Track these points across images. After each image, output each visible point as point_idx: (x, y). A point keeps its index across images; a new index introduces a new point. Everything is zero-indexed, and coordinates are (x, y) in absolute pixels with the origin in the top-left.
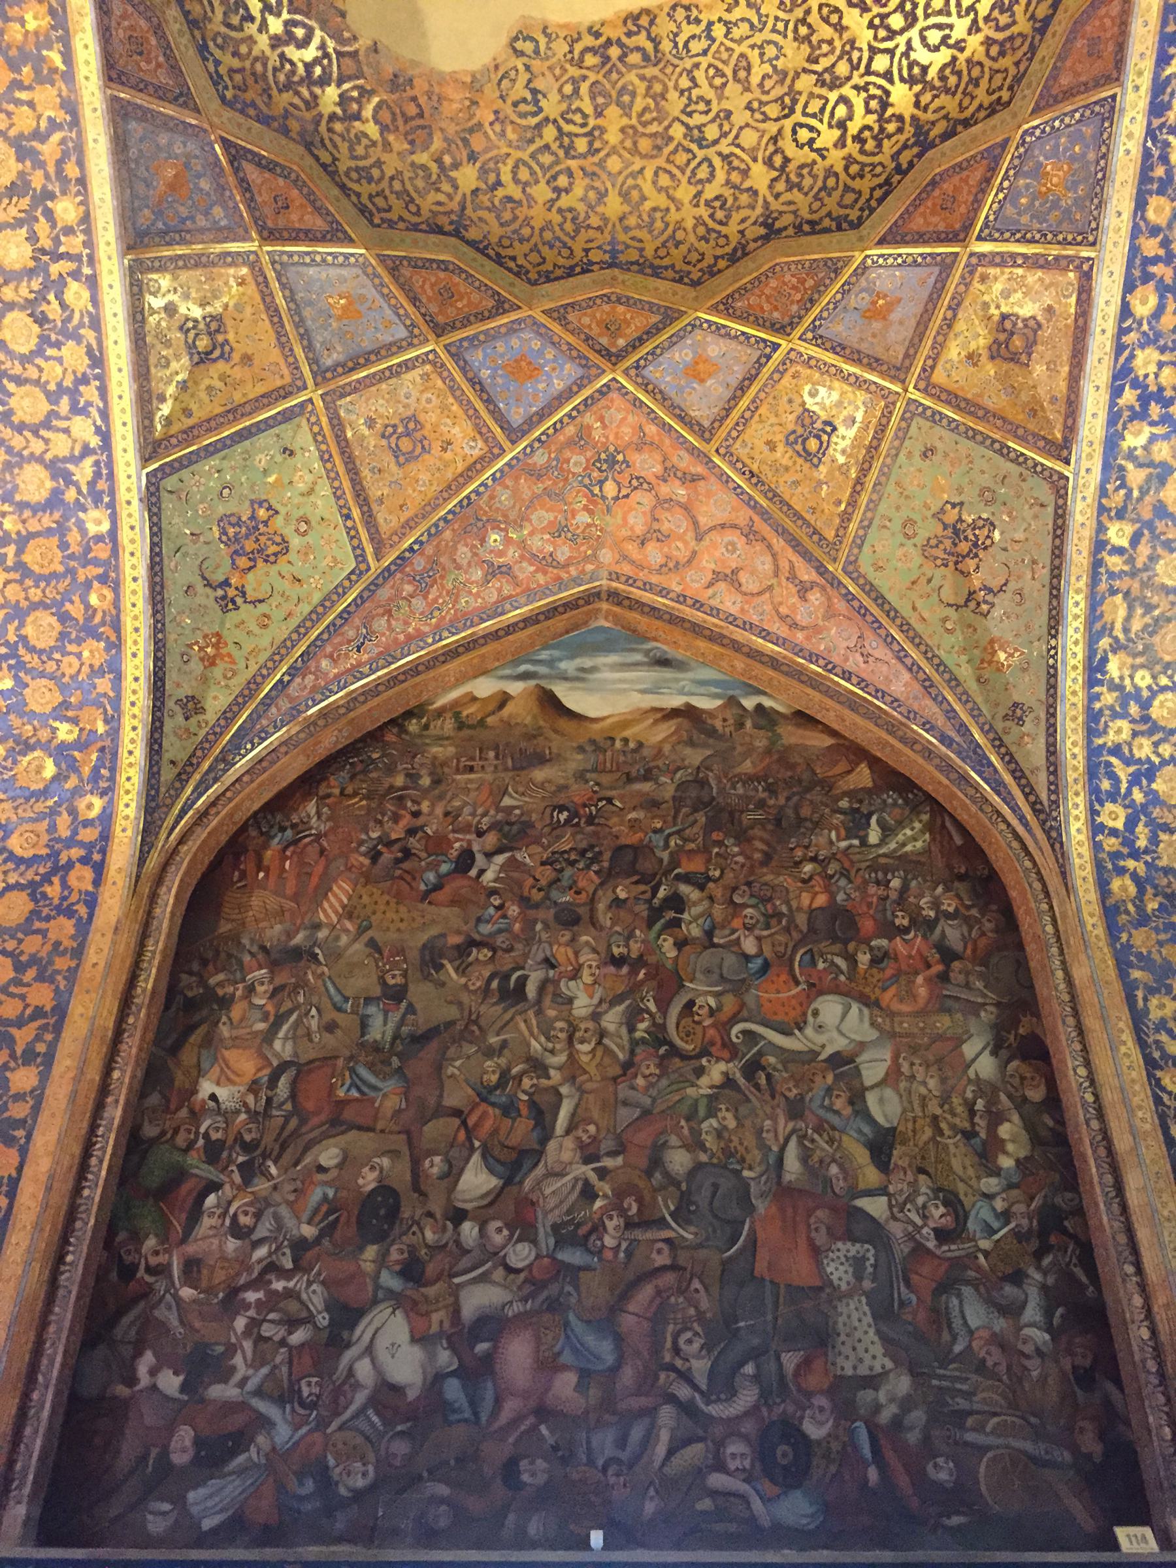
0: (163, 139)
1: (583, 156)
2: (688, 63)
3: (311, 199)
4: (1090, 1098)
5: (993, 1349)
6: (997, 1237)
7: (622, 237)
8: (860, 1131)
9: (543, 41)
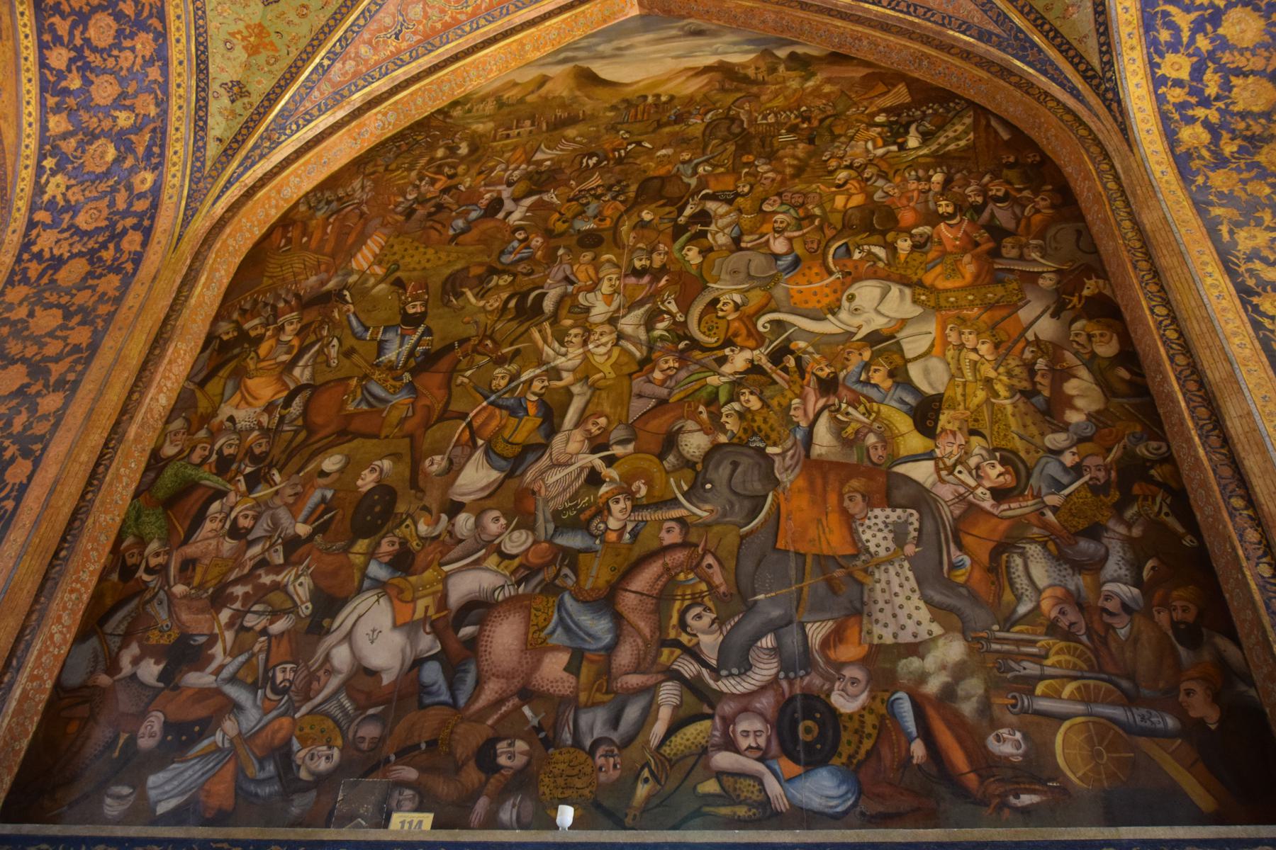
4: (1172, 335)
5: (1067, 608)
6: (1066, 492)
8: (902, 401)
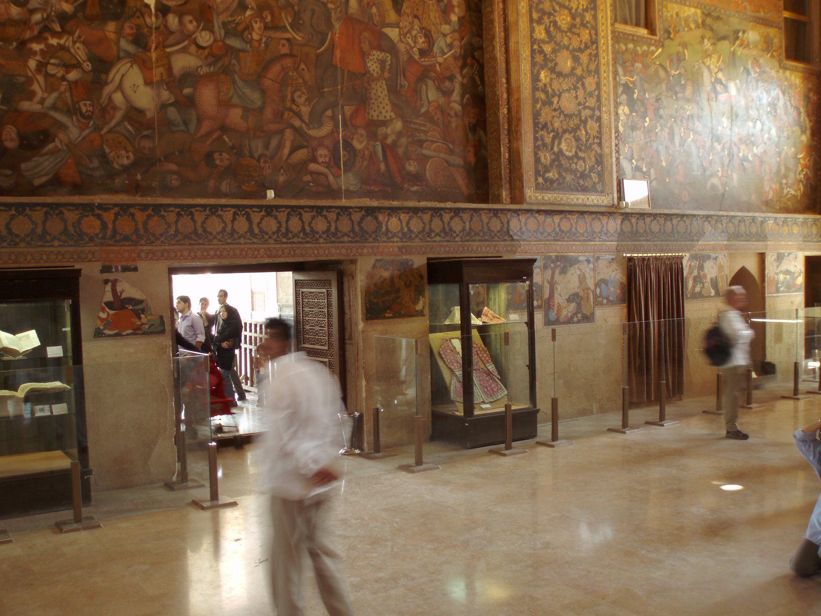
6: (445, 57)
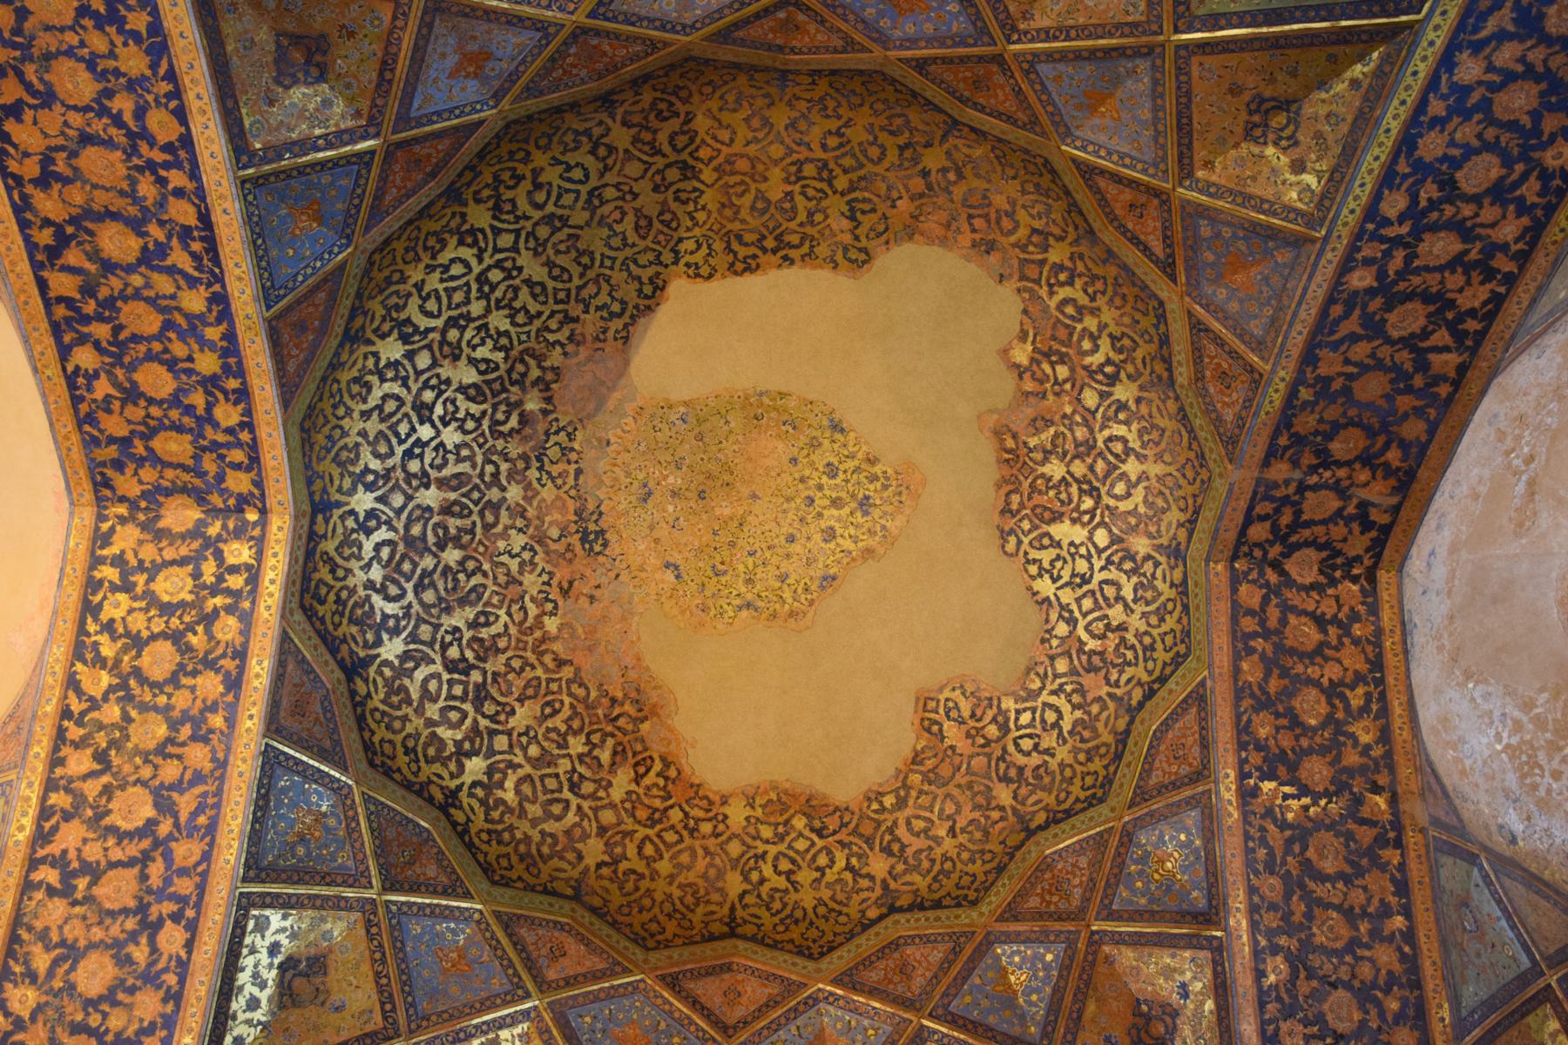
0: (1234, 307)
1: (808, 160)
2: (697, 231)
3: (1103, 202)
7: (773, 90)
9: (839, 257)
